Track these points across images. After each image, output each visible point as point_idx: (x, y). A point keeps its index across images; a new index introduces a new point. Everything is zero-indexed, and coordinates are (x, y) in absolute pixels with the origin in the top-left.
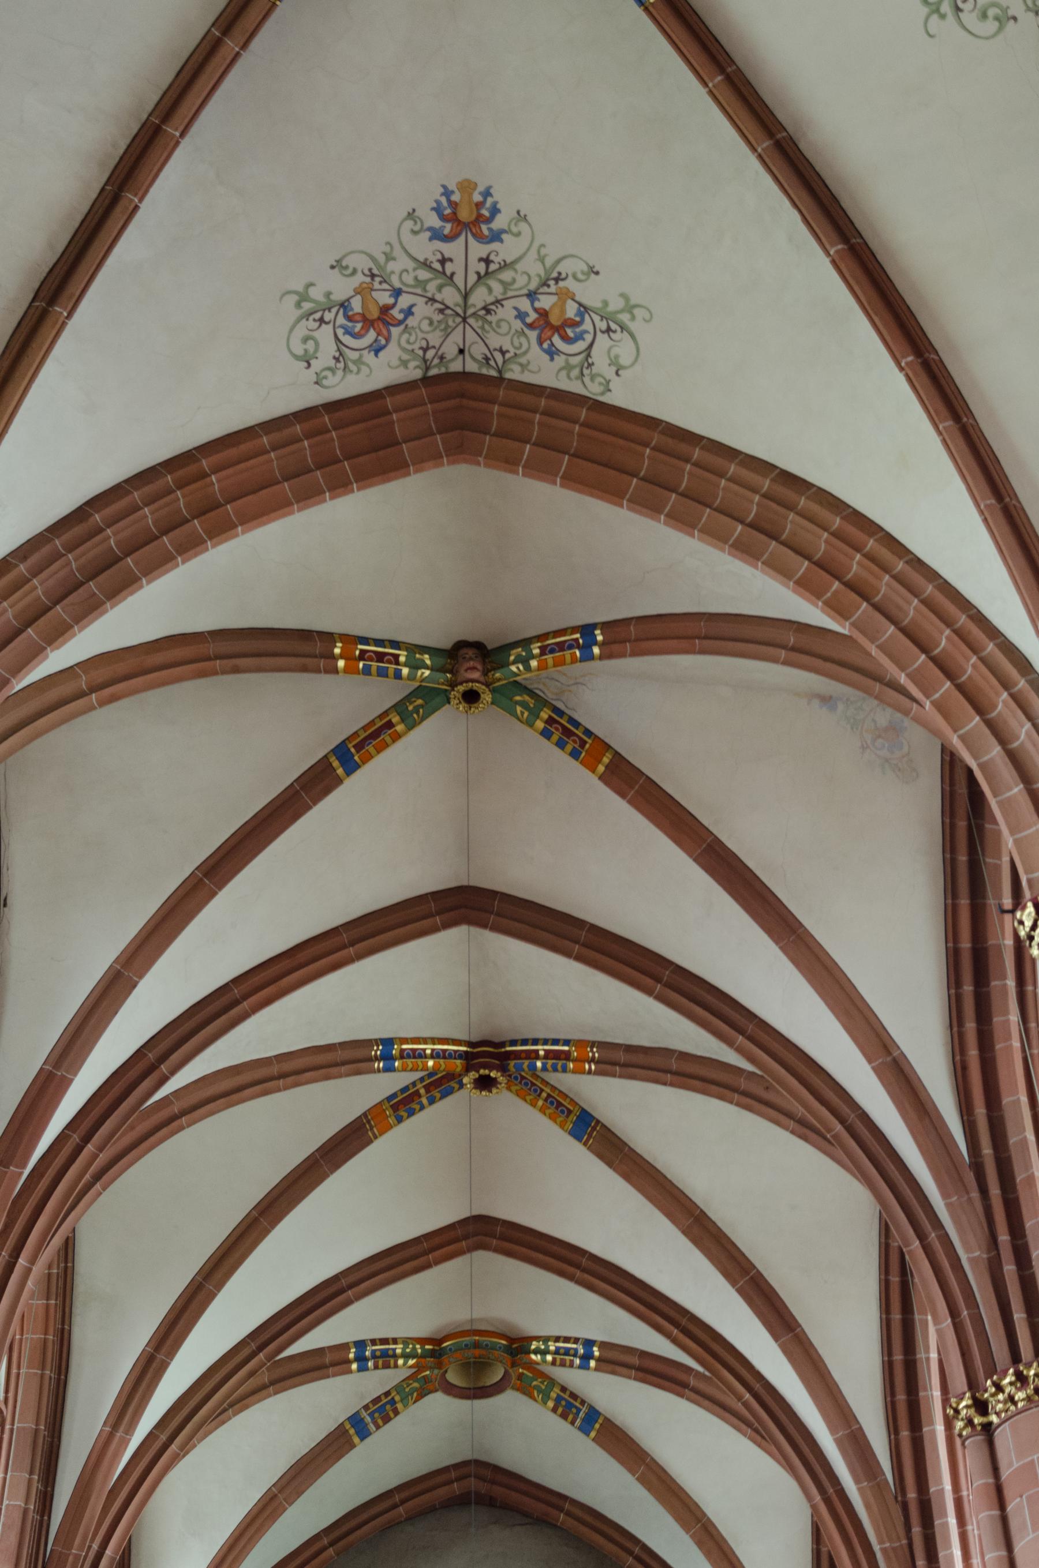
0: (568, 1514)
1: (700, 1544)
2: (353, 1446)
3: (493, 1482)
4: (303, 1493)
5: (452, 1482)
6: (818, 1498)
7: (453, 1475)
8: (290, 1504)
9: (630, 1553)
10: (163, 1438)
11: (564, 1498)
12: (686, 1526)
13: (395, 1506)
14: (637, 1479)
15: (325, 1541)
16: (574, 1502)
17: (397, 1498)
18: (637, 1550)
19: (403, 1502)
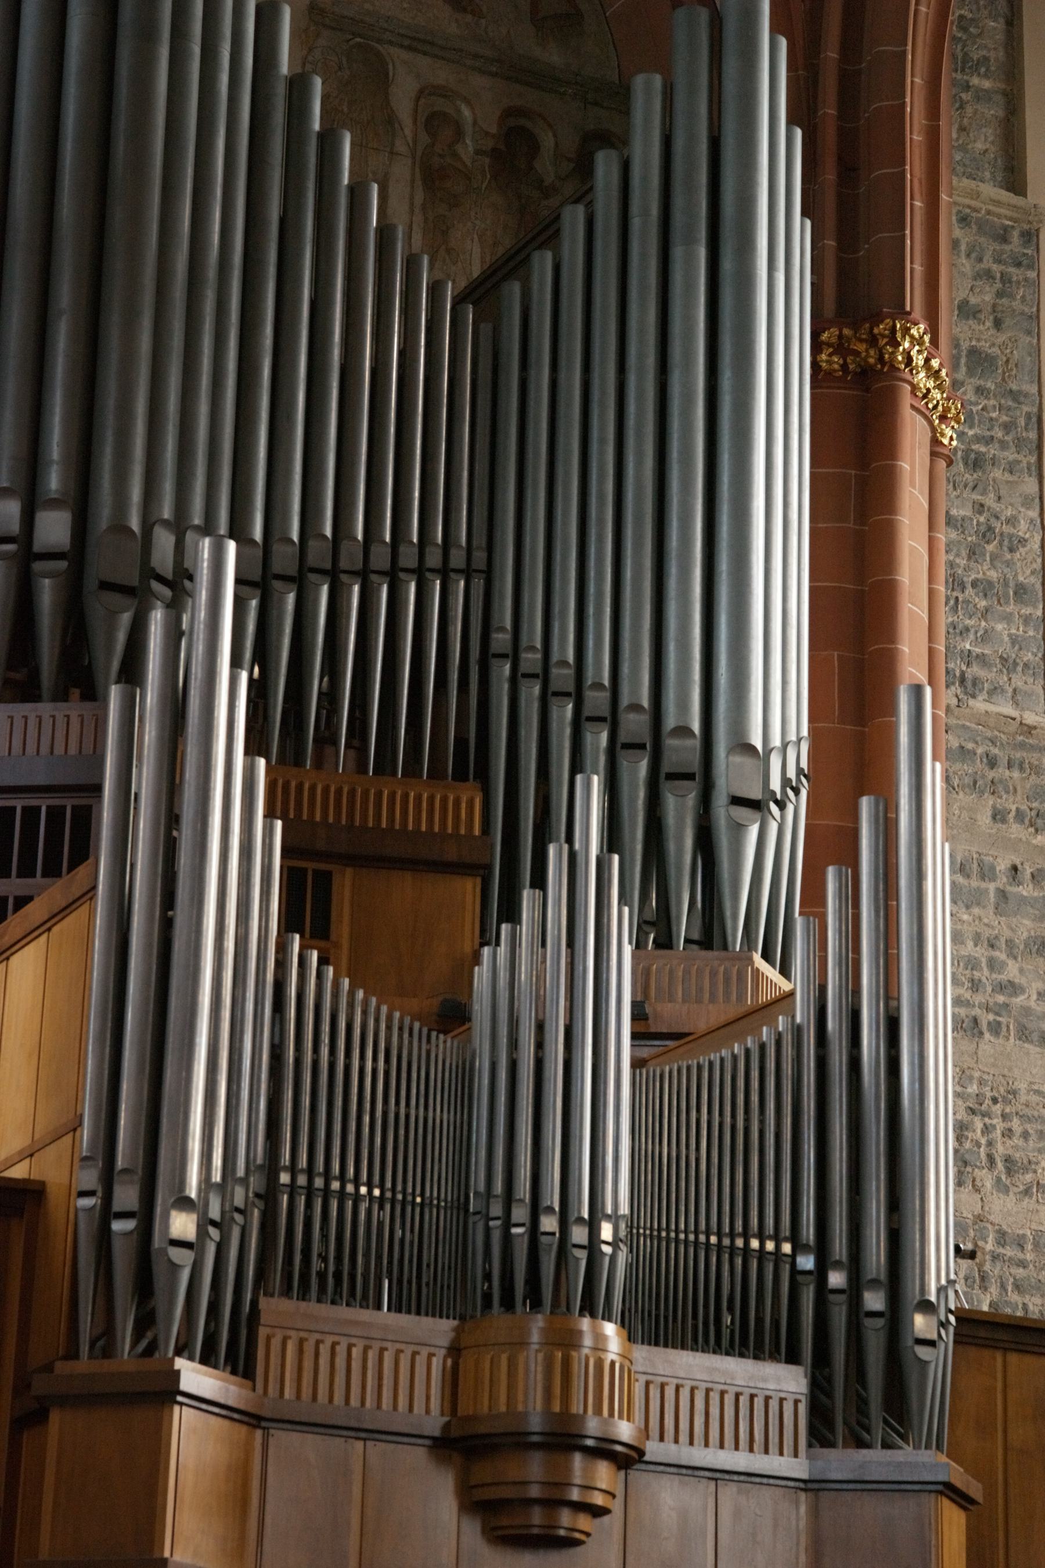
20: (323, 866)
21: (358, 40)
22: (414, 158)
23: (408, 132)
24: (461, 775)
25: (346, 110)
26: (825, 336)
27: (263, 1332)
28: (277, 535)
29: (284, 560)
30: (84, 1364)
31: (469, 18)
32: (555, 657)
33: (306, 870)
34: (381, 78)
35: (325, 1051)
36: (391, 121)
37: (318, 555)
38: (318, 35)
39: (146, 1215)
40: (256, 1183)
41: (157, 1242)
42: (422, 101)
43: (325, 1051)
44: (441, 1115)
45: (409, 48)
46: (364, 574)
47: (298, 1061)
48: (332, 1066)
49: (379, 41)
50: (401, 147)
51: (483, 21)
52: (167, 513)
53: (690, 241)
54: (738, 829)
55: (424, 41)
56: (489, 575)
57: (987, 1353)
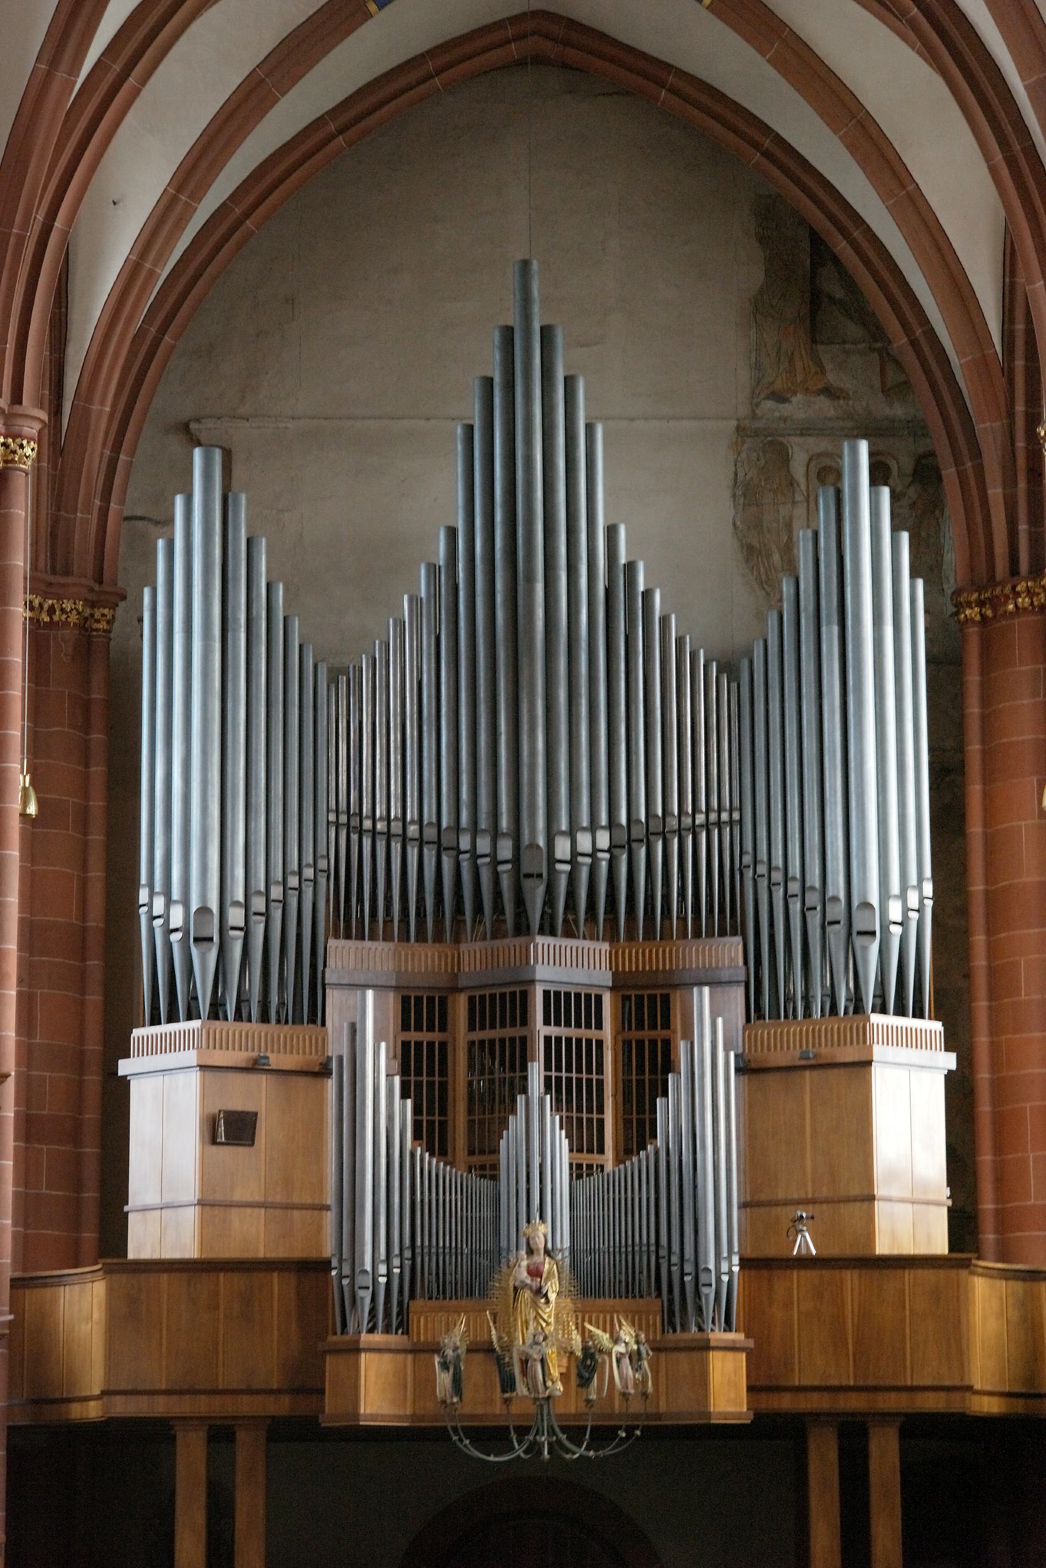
0: (672, 90)
1: (852, 148)
2: (368, 16)
3: (567, 43)
4: (300, 78)
5: (509, 42)
6: (999, 157)
7: (510, 33)
8: (283, 94)
9: (756, 146)
10: (117, 68)
11: (668, 67)
12: (833, 123)
13: (430, 77)
14: (769, 61)
15: (332, 127)
16: (681, 73)
17: (430, 66)
18: (767, 143)
19: (440, 71)
20: (665, 991)
21: (769, 439)
22: (808, 502)
23: (803, 487)
24: (734, 933)
25: (763, 483)
26: (1019, 588)
27: (411, 1315)
28: (634, 817)
29: (638, 832)
30: (338, 1338)
31: (841, 402)
32: (774, 864)
33: (655, 996)
34: (784, 458)
35: (434, 1195)
36: (792, 484)
37: (655, 826)
38: (743, 443)
39: (353, 1277)
40: (408, 1254)
41: (356, 1288)
42: (812, 464)
43: (434, 1195)
44: (487, 1213)
45: (802, 435)
46: (680, 832)
47: (422, 1201)
48: (437, 1200)
49: (783, 436)
50: (799, 497)
51: (851, 402)
52: (564, 826)
53: (829, 623)
54: (865, 949)
55: (809, 429)
56: (741, 821)
57: (788, 1272)
